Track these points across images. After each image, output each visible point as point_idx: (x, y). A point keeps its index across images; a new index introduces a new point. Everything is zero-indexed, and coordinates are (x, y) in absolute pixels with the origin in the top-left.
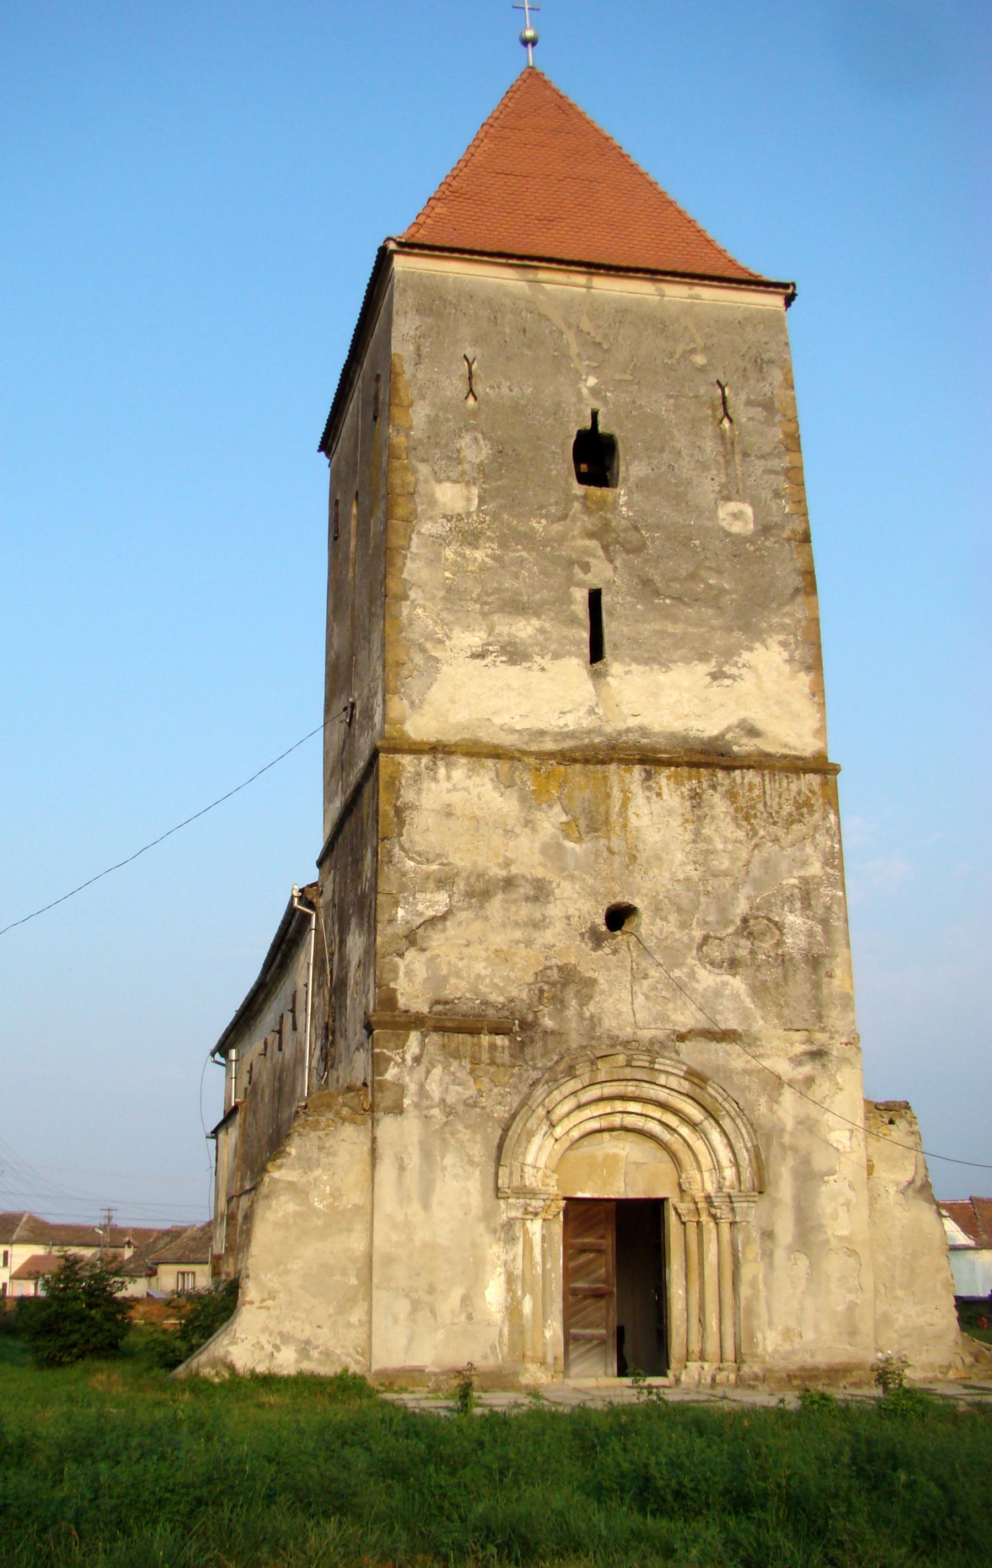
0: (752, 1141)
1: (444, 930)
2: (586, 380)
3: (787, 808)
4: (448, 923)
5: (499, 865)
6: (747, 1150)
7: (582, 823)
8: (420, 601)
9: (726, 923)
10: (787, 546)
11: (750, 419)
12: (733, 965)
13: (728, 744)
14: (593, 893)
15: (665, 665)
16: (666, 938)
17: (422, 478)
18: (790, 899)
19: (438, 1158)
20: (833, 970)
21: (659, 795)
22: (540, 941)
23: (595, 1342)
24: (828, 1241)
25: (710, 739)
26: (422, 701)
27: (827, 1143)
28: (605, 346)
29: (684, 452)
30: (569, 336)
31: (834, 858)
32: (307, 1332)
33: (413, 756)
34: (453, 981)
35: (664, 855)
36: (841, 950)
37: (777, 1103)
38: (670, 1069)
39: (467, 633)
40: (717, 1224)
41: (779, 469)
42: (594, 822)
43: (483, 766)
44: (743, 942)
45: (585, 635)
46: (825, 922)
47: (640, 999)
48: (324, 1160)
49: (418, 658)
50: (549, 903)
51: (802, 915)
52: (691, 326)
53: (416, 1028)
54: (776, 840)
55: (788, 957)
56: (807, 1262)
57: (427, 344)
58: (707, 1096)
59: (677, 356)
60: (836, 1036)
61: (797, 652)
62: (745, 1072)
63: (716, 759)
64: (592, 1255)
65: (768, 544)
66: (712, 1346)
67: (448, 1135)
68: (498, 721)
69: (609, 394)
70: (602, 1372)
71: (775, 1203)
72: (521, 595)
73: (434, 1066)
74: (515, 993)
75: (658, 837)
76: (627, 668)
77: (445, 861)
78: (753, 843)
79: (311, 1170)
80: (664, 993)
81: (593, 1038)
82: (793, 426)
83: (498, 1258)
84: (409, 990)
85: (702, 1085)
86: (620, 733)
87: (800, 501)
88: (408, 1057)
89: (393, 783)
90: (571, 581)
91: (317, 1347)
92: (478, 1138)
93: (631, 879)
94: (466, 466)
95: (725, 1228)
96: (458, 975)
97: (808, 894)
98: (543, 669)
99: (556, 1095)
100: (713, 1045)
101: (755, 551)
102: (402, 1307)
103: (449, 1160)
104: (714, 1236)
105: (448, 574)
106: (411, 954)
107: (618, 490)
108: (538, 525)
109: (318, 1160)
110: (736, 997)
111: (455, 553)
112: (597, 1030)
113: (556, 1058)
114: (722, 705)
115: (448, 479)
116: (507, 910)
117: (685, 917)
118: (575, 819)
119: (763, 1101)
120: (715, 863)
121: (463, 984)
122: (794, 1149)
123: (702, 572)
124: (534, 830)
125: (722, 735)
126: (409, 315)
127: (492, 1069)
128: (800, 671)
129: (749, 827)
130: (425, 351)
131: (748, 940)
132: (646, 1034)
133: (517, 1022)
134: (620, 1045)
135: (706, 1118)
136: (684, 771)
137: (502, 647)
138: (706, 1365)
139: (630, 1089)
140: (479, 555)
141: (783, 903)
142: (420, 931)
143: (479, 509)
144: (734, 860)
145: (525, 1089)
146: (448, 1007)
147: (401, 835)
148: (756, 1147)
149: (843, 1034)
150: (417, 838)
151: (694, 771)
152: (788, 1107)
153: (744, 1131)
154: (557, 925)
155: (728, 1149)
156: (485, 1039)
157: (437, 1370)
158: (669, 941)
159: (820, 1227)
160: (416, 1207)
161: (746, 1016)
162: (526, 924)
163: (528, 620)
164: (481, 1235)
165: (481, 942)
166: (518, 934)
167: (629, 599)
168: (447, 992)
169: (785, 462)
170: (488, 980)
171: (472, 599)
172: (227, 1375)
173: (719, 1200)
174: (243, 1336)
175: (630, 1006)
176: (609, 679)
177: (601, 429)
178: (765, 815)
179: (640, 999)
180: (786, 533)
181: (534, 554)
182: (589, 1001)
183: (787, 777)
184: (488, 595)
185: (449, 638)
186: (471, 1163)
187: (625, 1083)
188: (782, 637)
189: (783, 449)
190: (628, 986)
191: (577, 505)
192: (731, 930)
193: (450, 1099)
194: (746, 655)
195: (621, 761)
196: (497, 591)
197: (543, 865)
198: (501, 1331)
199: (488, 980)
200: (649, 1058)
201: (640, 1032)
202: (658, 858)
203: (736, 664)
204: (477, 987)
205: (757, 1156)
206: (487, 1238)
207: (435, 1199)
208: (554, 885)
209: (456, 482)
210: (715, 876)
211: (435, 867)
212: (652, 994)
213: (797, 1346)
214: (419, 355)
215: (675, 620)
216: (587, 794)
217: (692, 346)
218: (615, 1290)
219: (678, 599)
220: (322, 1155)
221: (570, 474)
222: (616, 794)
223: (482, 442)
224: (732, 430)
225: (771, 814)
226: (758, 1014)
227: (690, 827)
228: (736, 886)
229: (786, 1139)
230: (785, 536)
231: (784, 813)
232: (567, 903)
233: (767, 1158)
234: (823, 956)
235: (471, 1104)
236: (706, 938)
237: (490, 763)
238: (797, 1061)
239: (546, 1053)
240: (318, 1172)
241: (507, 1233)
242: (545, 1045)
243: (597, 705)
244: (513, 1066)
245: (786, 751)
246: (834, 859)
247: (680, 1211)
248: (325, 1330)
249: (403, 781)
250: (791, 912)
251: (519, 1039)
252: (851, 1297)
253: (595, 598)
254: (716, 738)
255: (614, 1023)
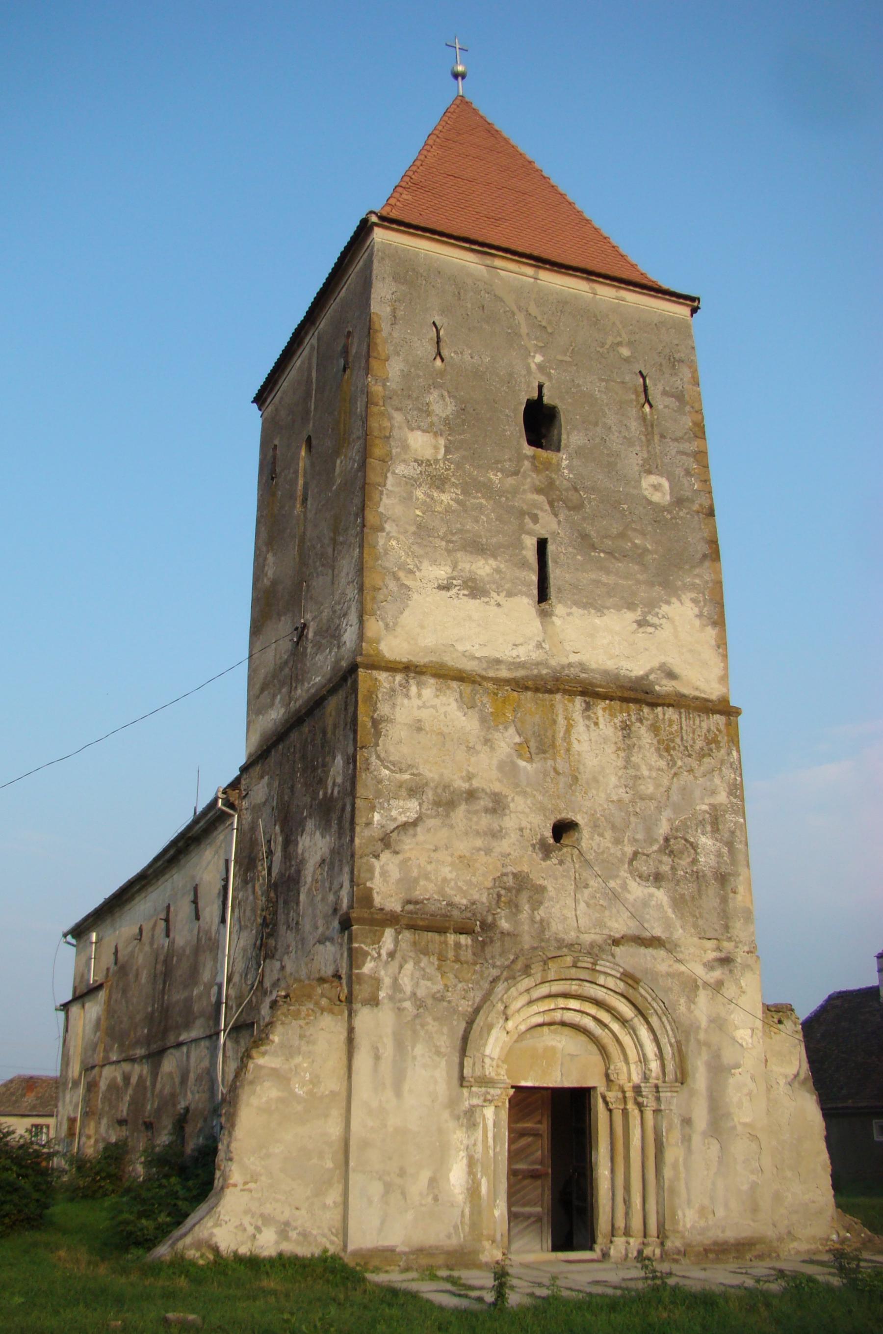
0: (675, 1037)
1: (415, 835)
2: (534, 357)
3: (700, 744)
4: (419, 829)
5: (462, 778)
6: (671, 1045)
7: (533, 744)
8: (394, 534)
9: (651, 840)
10: (696, 518)
11: (666, 407)
12: (658, 878)
13: (652, 684)
14: (542, 809)
15: (600, 610)
16: (603, 852)
17: (396, 424)
18: (702, 823)
19: (409, 1048)
20: (736, 887)
21: (596, 724)
22: (497, 850)
23: (532, 1219)
24: (734, 1128)
25: (636, 677)
26: (395, 624)
27: (734, 1039)
28: (550, 330)
29: (614, 428)
30: (520, 317)
31: (736, 789)
32: (286, 1214)
33: (388, 674)
34: (422, 883)
35: (601, 778)
36: (742, 870)
37: (694, 1003)
38: (609, 971)
39: (435, 567)
40: (641, 1112)
41: (689, 452)
42: (542, 744)
43: (449, 688)
44: (665, 859)
45: (535, 578)
46: (730, 845)
47: (582, 906)
48: (304, 1048)
49: (393, 585)
50: (505, 815)
51: (712, 837)
52: (618, 323)
53: (390, 926)
54: (691, 771)
55: (701, 874)
56: (718, 1146)
57: (402, 308)
58: (638, 996)
59: (607, 346)
60: (740, 945)
61: (706, 609)
62: (668, 974)
63: (642, 696)
64: (530, 1139)
65: (681, 514)
66: (636, 1223)
67: (418, 1027)
68: (460, 648)
69: (552, 371)
70: (539, 1247)
71: (692, 1093)
72: (480, 537)
73: (406, 962)
74: (476, 897)
75: (595, 762)
76: (569, 610)
77: (415, 772)
78: (672, 772)
79: (292, 1057)
80: (601, 902)
81: (542, 940)
82: (700, 417)
83: (461, 1142)
84: (382, 889)
85: (635, 986)
86: (563, 667)
87: (706, 481)
88: (384, 952)
89: (371, 697)
90: (522, 529)
91: (296, 1228)
92: (445, 1030)
93: (573, 798)
94: (435, 419)
95: (649, 1115)
96: (427, 877)
97: (716, 819)
98: (499, 605)
100: (642, 950)
101: (672, 518)
102: (376, 1189)
103: (420, 1049)
104: (638, 1121)
105: (418, 512)
106: (385, 856)
107: (560, 454)
108: (495, 477)
109: (299, 1048)
110: (660, 907)
111: (425, 494)
112: (547, 933)
113: (512, 957)
114: (646, 649)
115: (419, 428)
116: (470, 820)
117: (619, 832)
118: (527, 741)
119: (682, 1001)
120: (642, 787)
121: (431, 886)
122: (708, 1044)
123: (629, 533)
124: (492, 748)
125: (647, 675)
126: (387, 281)
127: (457, 966)
128: (707, 626)
129: (669, 758)
130: (400, 314)
131: (669, 858)
132: (587, 938)
133: (478, 923)
134: (566, 947)
135: (636, 1016)
136: (616, 704)
137: (464, 582)
138: (632, 1240)
139: (574, 987)
140: (445, 497)
141: (697, 825)
142: (394, 835)
143: (445, 459)
144: (658, 786)
145: (486, 986)
146: (418, 907)
147: (377, 745)
148: (678, 1042)
149: (745, 944)
150: (392, 749)
151: (624, 705)
152: (702, 1008)
153: (668, 1028)
154: (512, 835)
155: (654, 1044)
156: (451, 938)
157: (407, 1249)
158: (605, 855)
159: (728, 1115)
160: (389, 1093)
161: (668, 926)
162: (485, 834)
163: (486, 559)
164: (446, 1121)
165: (447, 848)
166: (479, 843)
167: (570, 549)
168: (417, 893)
169: (693, 447)
170: (453, 883)
171: (439, 536)
172: (211, 1257)
173: (647, 1090)
174: (227, 1218)
175: (574, 913)
176: (554, 618)
177: (546, 400)
178: (682, 748)
179: (582, 906)
180: (696, 507)
181: (492, 502)
182: (539, 906)
183: (699, 716)
184: (453, 534)
185: (420, 570)
186: (438, 1053)
187: (569, 982)
188: (693, 595)
189: (692, 435)
190: (572, 894)
191: (527, 464)
192: (655, 847)
193: (421, 993)
194: (665, 608)
195: (565, 692)
196: (461, 531)
197: (500, 781)
198: (463, 1212)
199: (453, 883)
200: (591, 960)
201: (582, 936)
202: (596, 780)
203: (657, 614)
204: (443, 889)
205: (680, 1051)
206: (452, 1124)
207: (406, 1087)
208: (509, 799)
209: (424, 431)
210: (642, 799)
211: (406, 776)
212: (592, 902)
213: (710, 1223)
214: (395, 317)
215: (608, 572)
216: (537, 719)
217: (619, 339)
218: (550, 1171)
219: (610, 553)
220: (303, 1043)
221: (520, 438)
222: (561, 720)
223: (447, 399)
224: (651, 414)
225: (686, 747)
226: (678, 923)
227: (622, 754)
228: (659, 809)
229: (702, 1036)
230: (695, 509)
231: (697, 747)
232: (521, 816)
234: (730, 874)
235: (439, 998)
236: (636, 854)
237: (454, 684)
238: (709, 967)
239: (503, 953)
240: (298, 1059)
241: (469, 1120)
242: (503, 945)
243: (544, 641)
244: (475, 964)
245: (697, 694)
246: (736, 790)
247: (608, 1099)
248: (303, 1212)
249: (380, 696)
250: (703, 834)
251: (480, 939)
252: (753, 1177)
253: (542, 545)
254: (642, 678)
255: (560, 927)
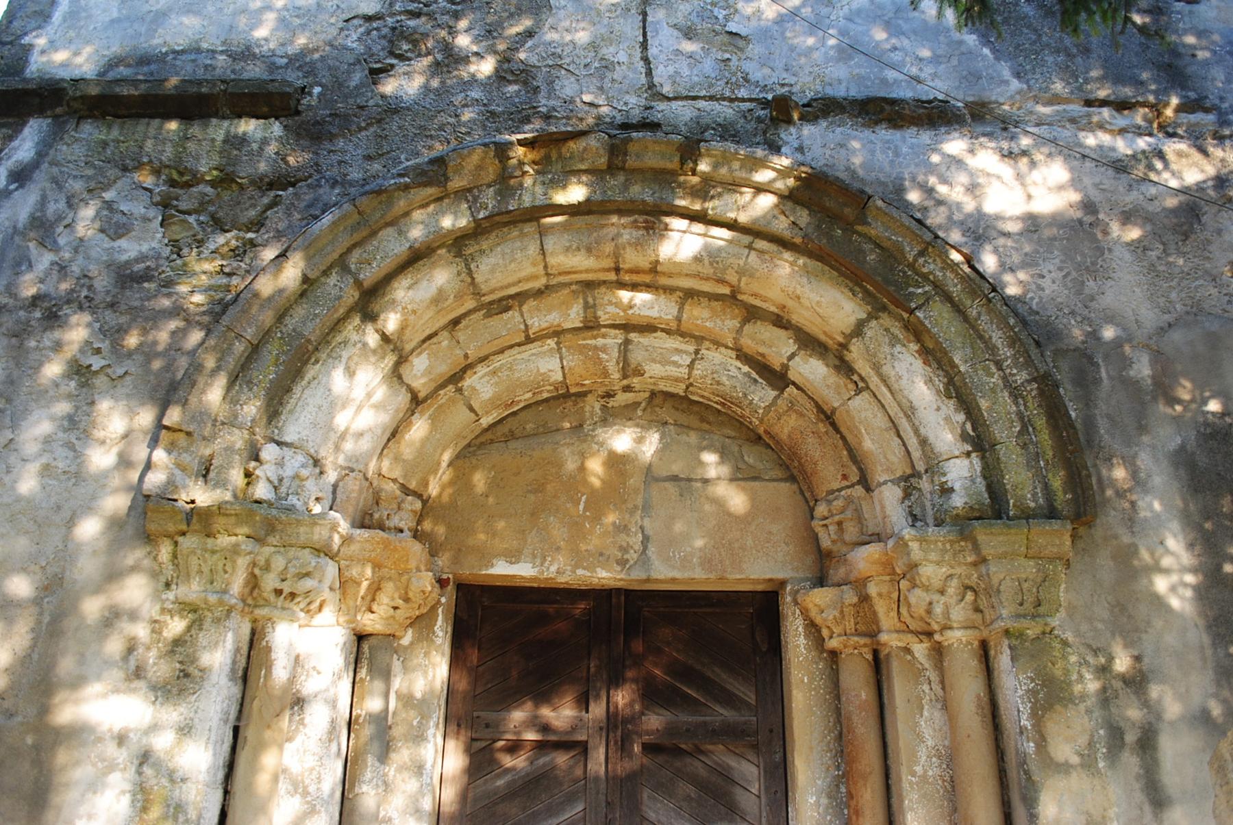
132: (682, 112)
153: (997, 337)
168: (156, 41)
233: (1090, 423)
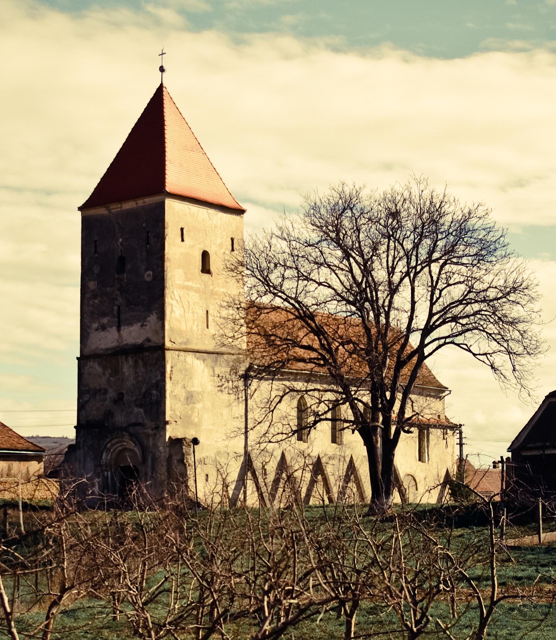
42: (116, 371)
99: (105, 443)
132: (124, 425)
140: (97, 301)
166: (101, 403)
179: (123, 417)
211: (87, 388)
222: (120, 363)
236: (136, 399)
238: (152, 430)
